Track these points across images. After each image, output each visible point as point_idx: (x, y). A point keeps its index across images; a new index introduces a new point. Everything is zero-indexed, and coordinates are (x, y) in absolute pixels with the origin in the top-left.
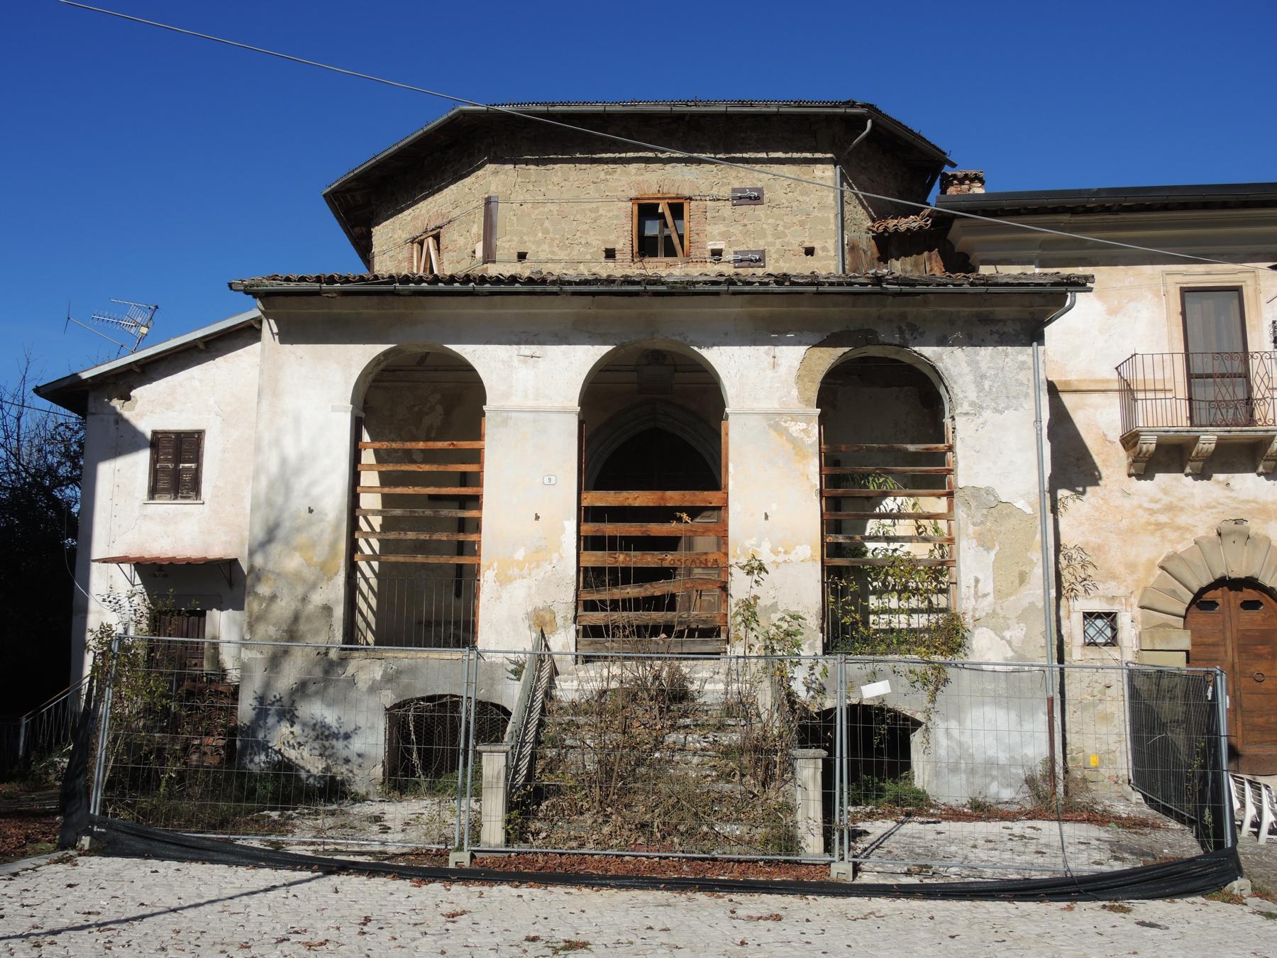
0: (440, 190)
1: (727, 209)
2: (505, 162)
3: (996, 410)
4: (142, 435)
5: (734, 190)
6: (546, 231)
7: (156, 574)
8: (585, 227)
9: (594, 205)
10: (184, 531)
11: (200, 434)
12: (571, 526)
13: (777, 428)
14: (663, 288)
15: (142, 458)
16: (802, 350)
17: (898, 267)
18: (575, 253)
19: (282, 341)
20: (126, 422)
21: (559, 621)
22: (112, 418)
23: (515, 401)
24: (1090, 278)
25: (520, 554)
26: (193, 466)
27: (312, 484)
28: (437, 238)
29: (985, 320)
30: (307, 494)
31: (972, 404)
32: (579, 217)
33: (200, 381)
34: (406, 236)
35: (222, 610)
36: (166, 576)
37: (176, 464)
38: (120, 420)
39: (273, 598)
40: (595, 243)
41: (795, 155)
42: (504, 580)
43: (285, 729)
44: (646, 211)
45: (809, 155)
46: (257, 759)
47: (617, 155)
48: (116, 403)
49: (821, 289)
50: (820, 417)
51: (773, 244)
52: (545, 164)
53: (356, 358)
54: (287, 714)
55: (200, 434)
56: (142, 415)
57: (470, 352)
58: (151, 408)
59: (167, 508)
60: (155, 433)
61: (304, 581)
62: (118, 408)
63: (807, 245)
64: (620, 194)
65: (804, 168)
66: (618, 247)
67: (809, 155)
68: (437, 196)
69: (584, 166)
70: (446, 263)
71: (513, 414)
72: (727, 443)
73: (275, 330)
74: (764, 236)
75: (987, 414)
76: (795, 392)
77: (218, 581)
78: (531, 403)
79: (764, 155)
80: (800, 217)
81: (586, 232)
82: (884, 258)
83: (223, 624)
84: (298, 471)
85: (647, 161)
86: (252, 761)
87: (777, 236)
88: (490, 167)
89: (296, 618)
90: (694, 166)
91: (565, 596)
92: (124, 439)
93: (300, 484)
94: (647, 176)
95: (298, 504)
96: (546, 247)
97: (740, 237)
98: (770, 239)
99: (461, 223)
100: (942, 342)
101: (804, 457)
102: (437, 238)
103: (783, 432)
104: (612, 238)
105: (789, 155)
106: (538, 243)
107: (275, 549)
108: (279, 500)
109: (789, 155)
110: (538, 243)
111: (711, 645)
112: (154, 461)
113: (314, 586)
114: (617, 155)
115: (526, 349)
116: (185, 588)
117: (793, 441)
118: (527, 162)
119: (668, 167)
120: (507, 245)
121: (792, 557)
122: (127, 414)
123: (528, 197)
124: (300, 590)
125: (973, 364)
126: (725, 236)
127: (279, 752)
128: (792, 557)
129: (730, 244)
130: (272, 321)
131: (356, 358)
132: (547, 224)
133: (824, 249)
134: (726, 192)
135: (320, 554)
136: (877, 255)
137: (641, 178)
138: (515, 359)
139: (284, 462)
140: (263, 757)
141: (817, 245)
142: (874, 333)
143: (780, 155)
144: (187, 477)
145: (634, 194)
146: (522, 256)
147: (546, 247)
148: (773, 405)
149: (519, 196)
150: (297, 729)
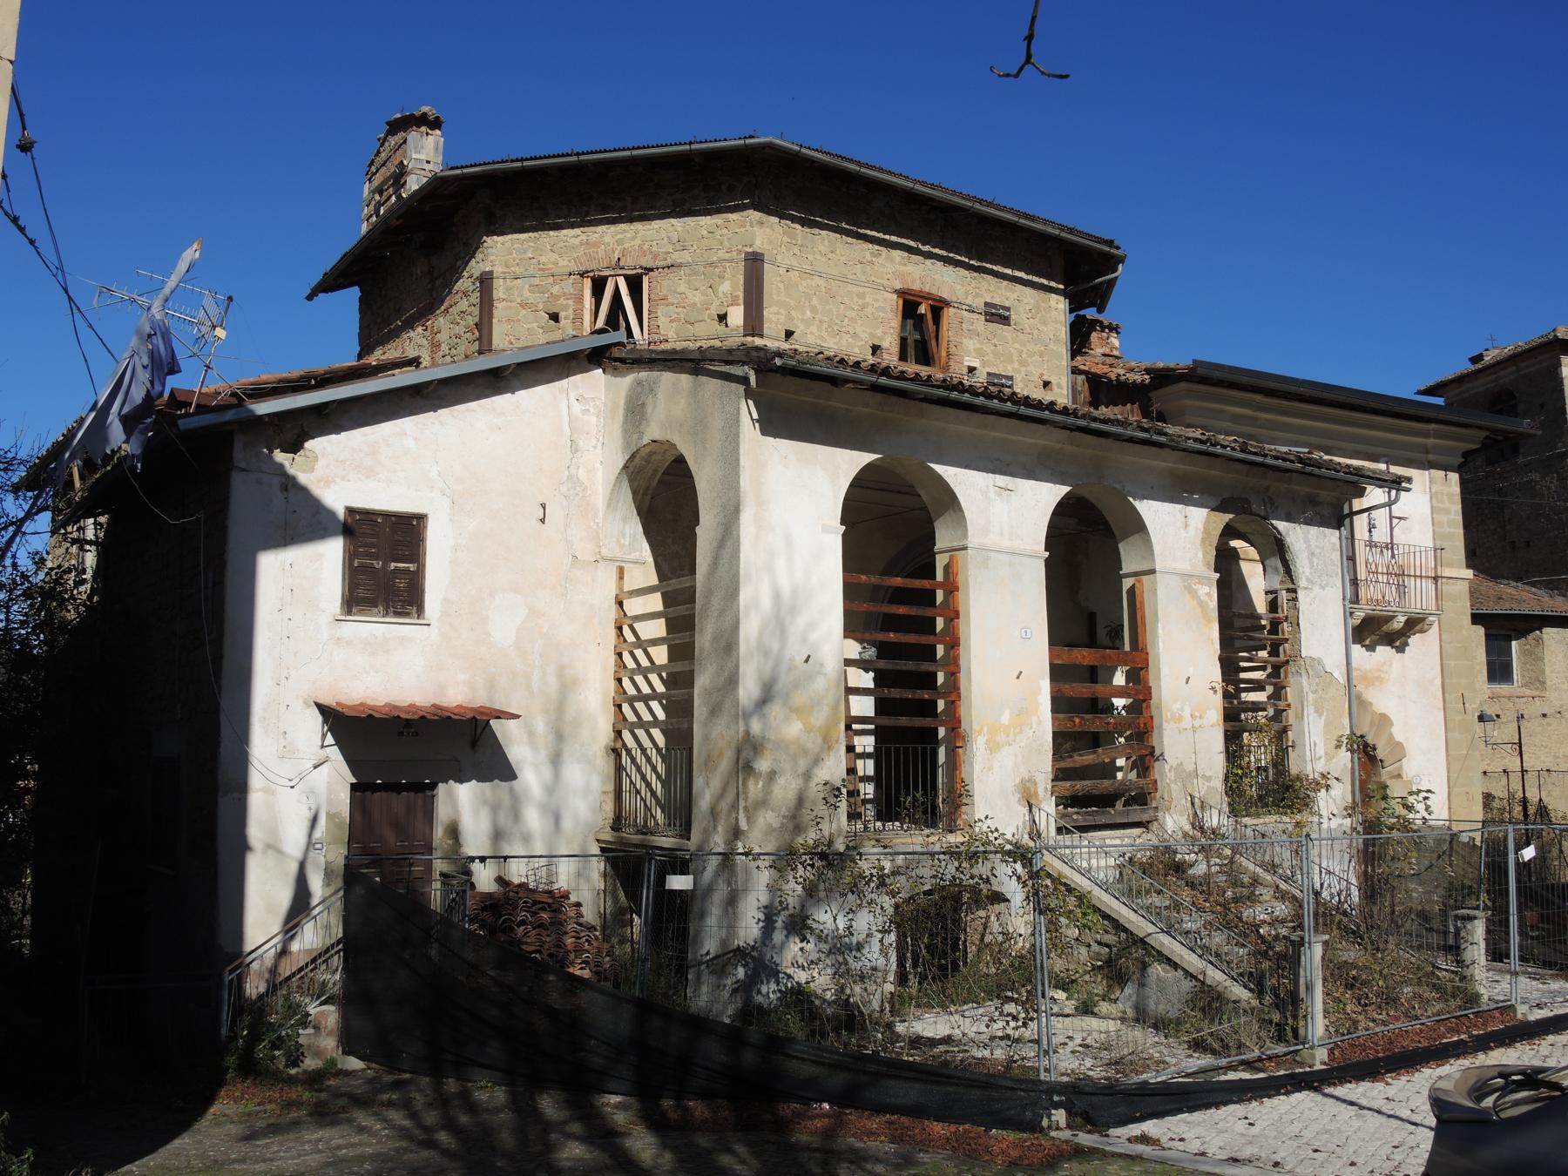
0: (631, 220)
1: (979, 322)
2: (770, 213)
3: (1323, 588)
4: (331, 514)
5: (987, 304)
6: (814, 310)
7: (350, 728)
8: (853, 314)
9: (861, 290)
10: (399, 667)
11: (421, 518)
12: (1045, 685)
13: (1189, 589)
14: (1163, 439)
15: (330, 554)
16: (1204, 512)
17: (1104, 411)
18: (844, 342)
19: (764, 432)
20: (304, 491)
21: (1041, 792)
22: (276, 480)
23: (992, 540)
24: (1409, 480)
25: (1005, 718)
26: (412, 567)
27: (811, 626)
28: (635, 284)
29: (1313, 501)
30: (804, 640)
31: (1308, 579)
32: (846, 300)
33: (416, 439)
34: (566, 264)
35: (461, 782)
36: (416, 734)
37: (386, 568)
38: (290, 485)
39: (772, 775)
40: (862, 335)
41: (1036, 279)
42: (993, 748)
43: (795, 946)
44: (910, 305)
45: (1045, 282)
46: (764, 989)
47: (881, 235)
48: (279, 456)
49: (1308, 469)
50: (1218, 582)
51: (1019, 372)
52: (811, 227)
53: (848, 463)
54: (799, 926)
55: (421, 518)
56: (328, 482)
57: (951, 474)
58: (346, 469)
59: (374, 629)
60: (351, 511)
61: (805, 752)
62: (287, 464)
63: (1046, 378)
64: (885, 282)
65: (1041, 294)
66: (885, 344)
67: (1045, 282)
68: (638, 226)
69: (850, 240)
70: (662, 321)
71: (993, 554)
72: (1142, 603)
73: (755, 416)
74: (1012, 362)
75: (1316, 588)
76: (1200, 555)
77: (460, 742)
78: (1005, 543)
79: (1009, 271)
80: (1017, 338)
81: (853, 320)
82: (1095, 403)
83: (463, 803)
84: (794, 610)
85: (909, 250)
86: (759, 992)
87: (1023, 363)
88: (754, 215)
89: (800, 801)
90: (951, 268)
91: (1043, 765)
92: (302, 519)
93: (801, 621)
94: (910, 268)
95: (795, 652)
96: (814, 329)
97: (991, 357)
98: (1016, 365)
99: (695, 273)
100: (1289, 518)
101: (1209, 621)
102: (635, 284)
103: (1194, 594)
104: (879, 332)
105: (1029, 277)
106: (807, 323)
107: (775, 710)
108: (776, 646)
109: (1029, 277)
110: (807, 323)
111: (1137, 814)
112: (350, 556)
113: (817, 761)
114: (881, 235)
115: (1002, 480)
116: (404, 756)
117: (1202, 604)
118: (793, 219)
119: (928, 262)
120: (774, 318)
121: (1204, 721)
122: (303, 478)
123: (795, 263)
124: (803, 764)
125: (1307, 540)
126: (980, 353)
127: (789, 976)
128: (1204, 721)
129: (984, 364)
130: (751, 402)
131: (848, 463)
132: (815, 301)
133: (1059, 385)
134: (979, 304)
135: (820, 718)
136: (1089, 399)
137: (903, 268)
138: (992, 489)
139: (777, 596)
140: (773, 986)
141: (1054, 380)
142: (1248, 502)
143: (1022, 275)
144: (402, 584)
145: (898, 286)
146: (789, 334)
147: (814, 329)
148: (1184, 566)
149: (786, 260)
150: (810, 947)
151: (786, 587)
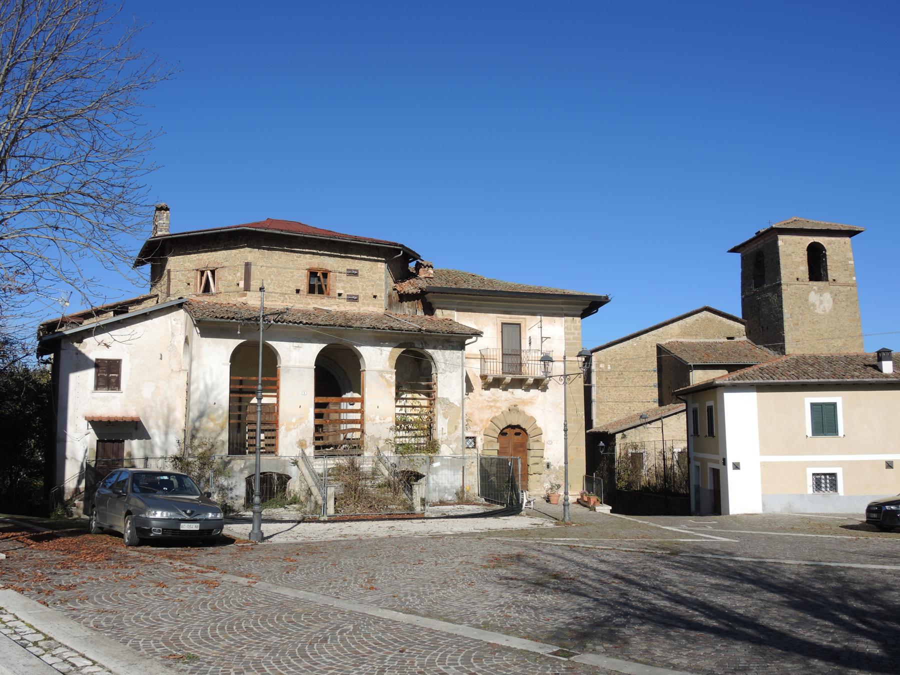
1: (344, 277)
4: (91, 361)
6: (272, 280)
7: (97, 424)
10: (113, 405)
11: (120, 361)
13: (382, 376)
15: (91, 373)
16: (390, 349)
19: (202, 336)
20: (83, 355)
21: (308, 444)
25: (294, 420)
27: (218, 394)
28: (213, 272)
34: (193, 266)
37: (108, 375)
38: (79, 353)
42: (288, 430)
44: (313, 274)
48: (76, 345)
55: (120, 361)
56: (90, 351)
59: (104, 394)
60: (97, 360)
68: (214, 253)
70: (220, 286)
74: (358, 289)
75: (447, 373)
78: (297, 364)
83: (133, 447)
84: (212, 390)
85: (314, 254)
88: (248, 249)
92: (82, 363)
93: (214, 394)
94: (313, 260)
100: (435, 348)
102: (213, 272)
106: (269, 284)
107: (204, 420)
108: (205, 400)
110: (269, 284)
112: (97, 373)
115: (296, 344)
116: (113, 433)
117: (387, 381)
118: (264, 249)
122: (83, 351)
125: (443, 355)
126: (344, 288)
131: (232, 344)
139: (206, 386)
141: (378, 295)
144: (113, 380)
145: (308, 267)
148: (380, 368)
151: (209, 383)
